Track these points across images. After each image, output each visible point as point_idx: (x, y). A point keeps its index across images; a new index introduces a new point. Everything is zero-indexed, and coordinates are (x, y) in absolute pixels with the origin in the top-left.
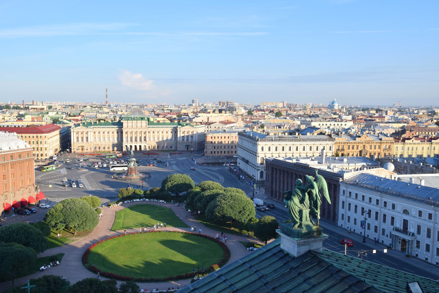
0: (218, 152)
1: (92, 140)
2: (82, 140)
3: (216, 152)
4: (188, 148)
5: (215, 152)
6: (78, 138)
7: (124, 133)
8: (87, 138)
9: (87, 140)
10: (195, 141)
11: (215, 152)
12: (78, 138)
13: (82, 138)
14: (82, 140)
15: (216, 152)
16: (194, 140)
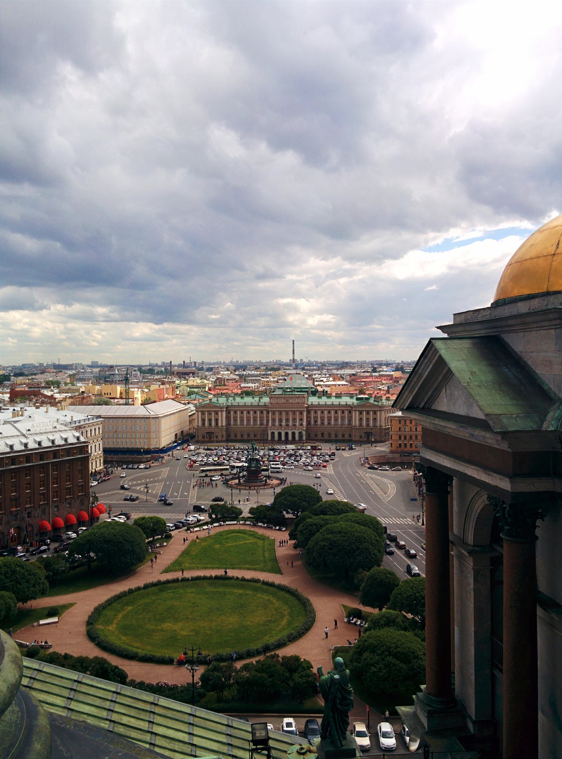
0: (411, 444)
1: (224, 424)
2: (210, 424)
3: (408, 446)
4: (368, 438)
5: (406, 444)
6: (203, 420)
7: (270, 413)
8: (217, 420)
9: (217, 424)
10: (380, 426)
11: (406, 444)
12: (203, 420)
13: (210, 420)
14: (210, 424)
15: (408, 446)
16: (378, 424)
